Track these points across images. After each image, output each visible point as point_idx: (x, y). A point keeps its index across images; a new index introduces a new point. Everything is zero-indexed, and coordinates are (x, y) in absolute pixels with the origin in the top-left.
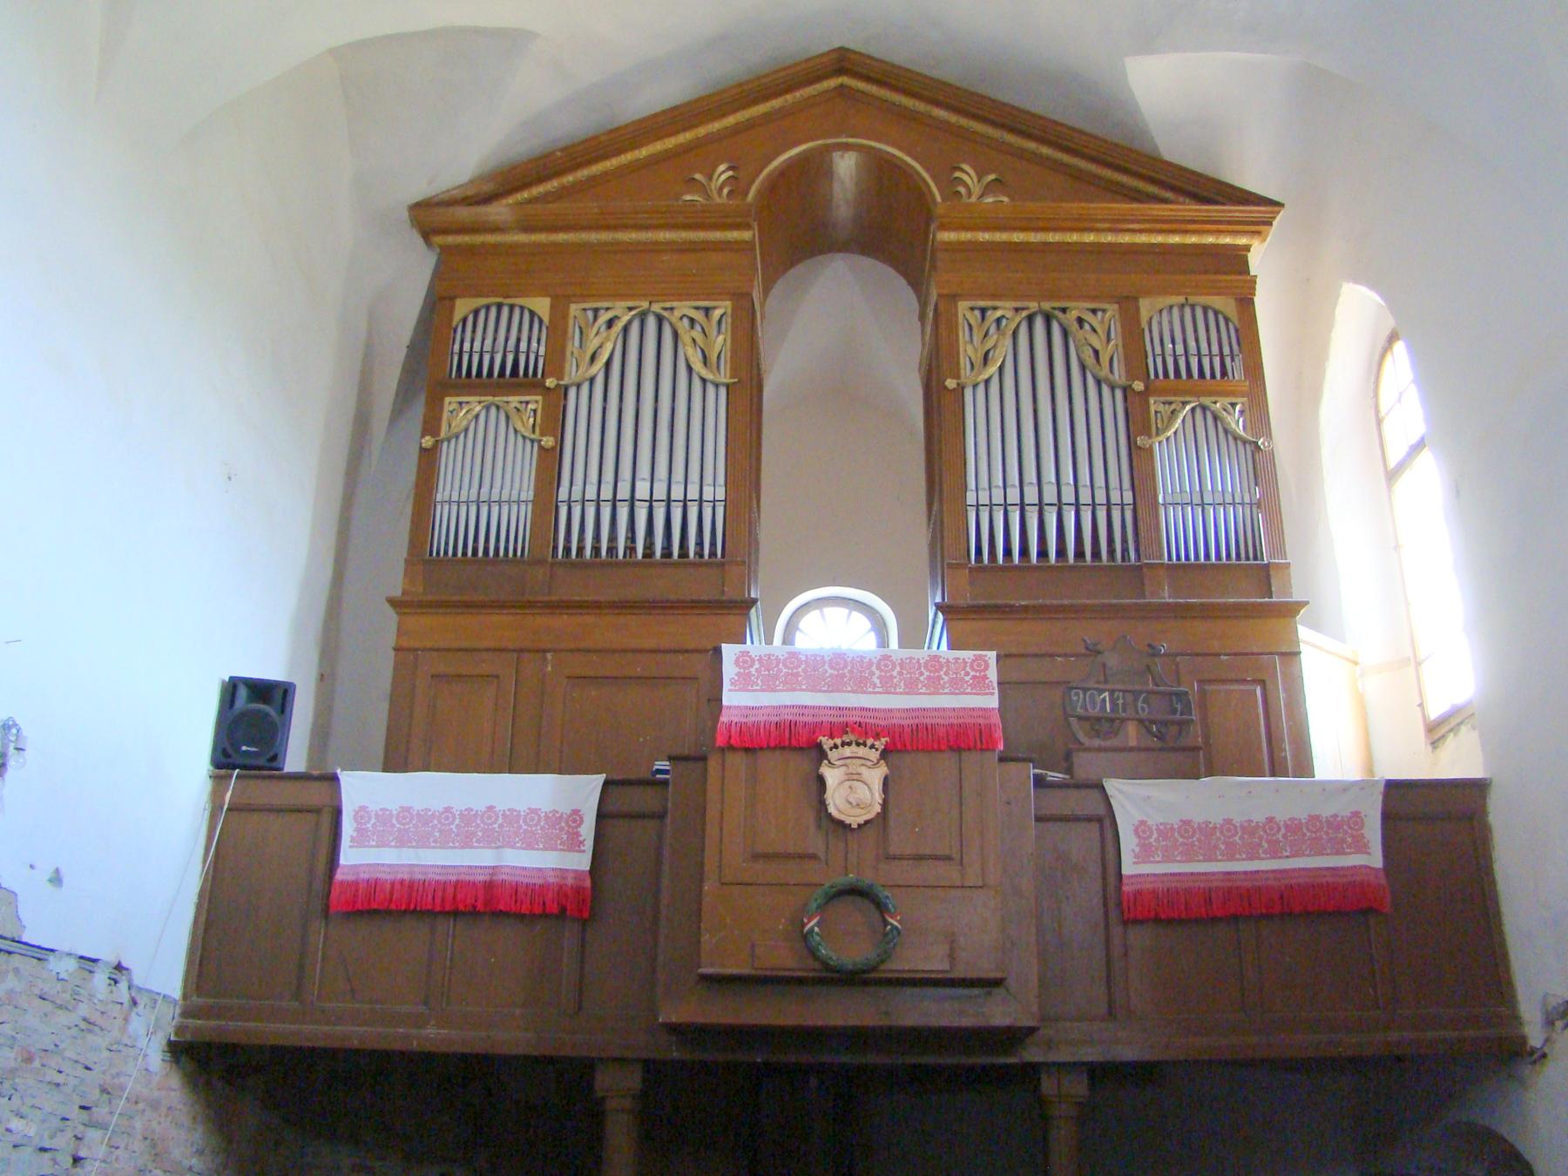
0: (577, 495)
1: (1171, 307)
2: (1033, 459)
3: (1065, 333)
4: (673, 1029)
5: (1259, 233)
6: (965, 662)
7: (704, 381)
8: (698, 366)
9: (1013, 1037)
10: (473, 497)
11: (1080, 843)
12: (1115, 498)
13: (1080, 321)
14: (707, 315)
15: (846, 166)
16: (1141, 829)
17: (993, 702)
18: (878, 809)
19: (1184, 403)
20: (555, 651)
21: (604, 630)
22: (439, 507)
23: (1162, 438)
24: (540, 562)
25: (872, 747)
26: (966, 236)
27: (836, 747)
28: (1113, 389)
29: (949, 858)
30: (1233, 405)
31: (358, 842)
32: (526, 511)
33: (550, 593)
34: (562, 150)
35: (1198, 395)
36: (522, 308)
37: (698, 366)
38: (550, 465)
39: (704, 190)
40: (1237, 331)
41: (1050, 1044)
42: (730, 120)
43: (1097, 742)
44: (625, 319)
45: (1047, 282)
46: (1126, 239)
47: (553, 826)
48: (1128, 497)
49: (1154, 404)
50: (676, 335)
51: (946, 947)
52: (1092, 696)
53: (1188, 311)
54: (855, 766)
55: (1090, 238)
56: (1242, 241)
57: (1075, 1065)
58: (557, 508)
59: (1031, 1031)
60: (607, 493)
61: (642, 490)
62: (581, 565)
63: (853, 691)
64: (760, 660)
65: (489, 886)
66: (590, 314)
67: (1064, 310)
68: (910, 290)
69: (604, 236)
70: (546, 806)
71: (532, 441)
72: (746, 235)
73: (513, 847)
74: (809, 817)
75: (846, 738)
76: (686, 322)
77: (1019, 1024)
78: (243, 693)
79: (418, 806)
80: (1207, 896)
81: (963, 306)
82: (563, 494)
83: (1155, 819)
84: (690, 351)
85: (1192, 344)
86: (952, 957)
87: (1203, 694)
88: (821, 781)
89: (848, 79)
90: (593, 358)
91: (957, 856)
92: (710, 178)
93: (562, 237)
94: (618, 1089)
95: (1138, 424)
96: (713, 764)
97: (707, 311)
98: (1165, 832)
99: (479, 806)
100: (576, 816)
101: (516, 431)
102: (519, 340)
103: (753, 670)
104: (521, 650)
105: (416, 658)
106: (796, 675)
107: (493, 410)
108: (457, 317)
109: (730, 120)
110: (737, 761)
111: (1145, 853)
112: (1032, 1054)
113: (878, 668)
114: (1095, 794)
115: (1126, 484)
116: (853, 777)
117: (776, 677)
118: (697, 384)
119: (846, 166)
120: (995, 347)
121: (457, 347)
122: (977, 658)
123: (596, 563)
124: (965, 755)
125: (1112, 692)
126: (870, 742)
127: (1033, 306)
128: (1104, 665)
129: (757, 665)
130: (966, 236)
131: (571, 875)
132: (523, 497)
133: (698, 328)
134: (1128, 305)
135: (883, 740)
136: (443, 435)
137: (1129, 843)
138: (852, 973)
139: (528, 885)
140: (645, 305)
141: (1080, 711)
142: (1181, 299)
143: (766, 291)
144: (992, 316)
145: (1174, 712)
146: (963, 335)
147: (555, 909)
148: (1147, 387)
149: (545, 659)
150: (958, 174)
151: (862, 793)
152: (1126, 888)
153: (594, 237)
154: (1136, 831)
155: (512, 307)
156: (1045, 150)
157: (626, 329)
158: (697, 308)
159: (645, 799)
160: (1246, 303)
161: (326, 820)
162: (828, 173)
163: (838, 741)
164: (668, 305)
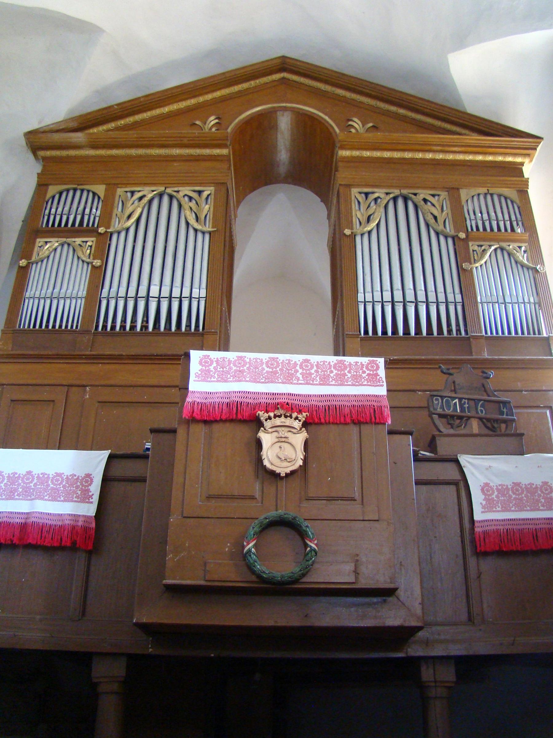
1: (479, 195)
2: (399, 274)
3: (416, 207)
4: (145, 628)
5: (528, 155)
6: (362, 365)
7: (196, 231)
8: (192, 221)
9: (403, 635)
10: (49, 295)
12: (451, 298)
13: (425, 200)
14: (200, 195)
15: (285, 122)
16: (485, 489)
17: (382, 391)
18: (301, 463)
19: (490, 246)
20: (91, 386)
21: (124, 374)
22: (27, 301)
23: (478, 265)
24: (87, 332)
25: (296, 418)
26: (356, 153)
27: (270, 418)
28: (446, 237)
29: (353, 499)
30: (520, 247)
32: (81, 303)
33: (91, 351)
34: (118, 105)
35: (498, 241)
36: (88, 191)
37: (192, 221)
38: (98, 277)
40: (519, 208)
41: (427, 643)
42: (218, 94)
43: (452, 431)
44: (150, 196)
45: (406, 182)
46: (451, 157)
47: (71, 485)
48: (459, 298)
49: (473, 246)
50: (180, 206)
51: (353, 565)
52: (447, 401)
53: (489, 197)
54: (284, 432)
55: (430, 156)
58: (100, 301)
59: (414, 630)
60: (132, 293)
61: (155, 291)
63: (283, 383)
64: (217, 361)
65: (24, 527)
66: (129, 195)
67: (415, 194)
68: (322, 205)
69: (141, 152)
71: (88, 263)
72: (225, 151)
73: (43, 499)
74: (250, 469)
75: (277, 412)
76: (186, 199)
77: (407, 624)
80: (535, 535)
81: (355, 191)
83: (495, 482)
84: (188, 213)
85: (492, 214)
86: (356, 572)
88: (259, 444)
89: (287, 72)
90: (129, 217)
91: (357, 495)
92: (205, 123)
93: (114, 152)
94: (108, 674)
95: (463, 256)
97: (200, 193)
98: (502, 490)
99: (22, 471)
100: (88, 478)
101: (78, 258)
102: (85, 208)
103: (212, 368)
104: (72, 386)
105: (3, 389)
106: (242, 372)
107: (66, 246)
108: (49, 195)
109: (218, 94)
110: (199, 430)
111: (489, 506)
112: (414, 650)
113: (301, 367)
114: (451, 467)
115: (457, 290)
117: (228, 373)
118: (191, 232)
119: (285, 122)
120: (374, 213)
121: (47, 212)
122: (371, 362)
124: (363, 427)
125: (460, 399)
126: (295, 415)
127: (397, 192)
128: (454, 382)
129: (215, 364)
130: (356, 153)
131: (81, 519)
132: (80, 295)
133: (194, 202)
134: (453, 192)
135: (304, 414)
136: (33, 259)
138: (282, 583)
139: (51, 526)
140: (162, 189)
141: (439, 411)
142: (483, 190)
143: (239, 203)
144: (372, 197)
145: (502, 413)
146: (355, 206)
147: (68, 544)
148: (467, 236)
149: (85, 391)
150: (350, 123)
151: (288, 451)
152: (477, 530)
153: (133, 152)
154: (482, 490)
155: (82, 191)
156: (402, 111)
158: (194, 191)
160: (523, 193)
162: (274, 127)
163: (272, 414)
164: (176, 189)
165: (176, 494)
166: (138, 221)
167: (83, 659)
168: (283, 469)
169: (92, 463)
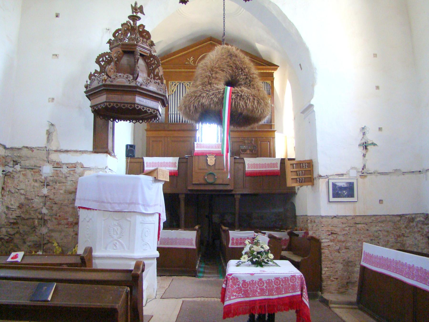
0: (171, 113)
4: (189, 190)
11: (240, 166)
16: (248, 164)
24: (166, 124)
31: (147, 166)
39: (189, 62)
54: (211, 158)
56: (273, 71)
57: (239, 194)
62: (173, 124)
70: (171, 161)
78: (129, 146)
79: (154, 162)
82: (169, 113)
83: (250, 163)
87: (261, 143)
94: (182, 197)
96: (194, 157)
98: (251, 165)
100: (175, 163)
110: (197, 157)
111: (249, 168)
112: (233, 193)
116: (211, 159)
123: (174, 124)
137: (247, 166)
151: (212, 162)
157: (177, 86)
159: (185, 160)
160: (272, 82)
161: (142, 163)
165: (194, 169)
166: (175, 92)
167: (178, 194)
168: (211, 164)
169: (175, 160)
